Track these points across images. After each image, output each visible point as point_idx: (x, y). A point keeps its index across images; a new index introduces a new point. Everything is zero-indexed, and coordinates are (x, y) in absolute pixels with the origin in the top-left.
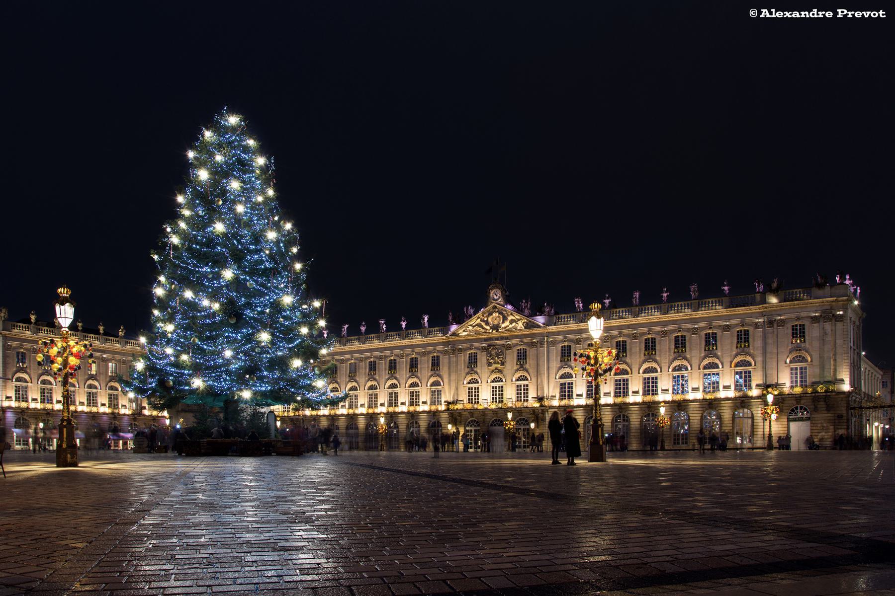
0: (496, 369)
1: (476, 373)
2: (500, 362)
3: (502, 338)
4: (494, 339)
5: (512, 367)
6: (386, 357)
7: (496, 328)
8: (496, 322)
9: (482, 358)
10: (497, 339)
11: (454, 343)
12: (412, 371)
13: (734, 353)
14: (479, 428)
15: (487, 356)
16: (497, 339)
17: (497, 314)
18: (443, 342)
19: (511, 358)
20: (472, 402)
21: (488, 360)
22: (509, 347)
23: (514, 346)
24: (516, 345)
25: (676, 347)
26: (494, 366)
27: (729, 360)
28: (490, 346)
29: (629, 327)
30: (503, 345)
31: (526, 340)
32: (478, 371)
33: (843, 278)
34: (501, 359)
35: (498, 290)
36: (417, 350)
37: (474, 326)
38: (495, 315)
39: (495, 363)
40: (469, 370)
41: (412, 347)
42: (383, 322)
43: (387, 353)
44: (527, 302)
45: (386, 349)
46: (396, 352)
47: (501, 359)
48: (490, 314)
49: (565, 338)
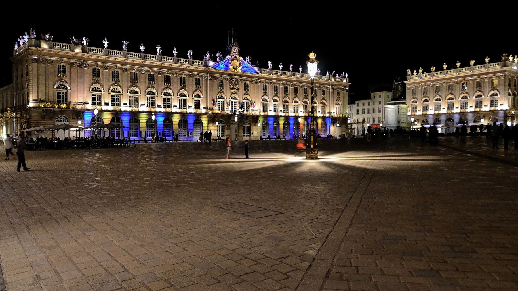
0: (234, 92)
1: (223, 92)
2: (236, 88)
3: (238, 75)
4: (233, 75)
5: (243, 92)
6: (163, 73)
7: (235, 69)
8: (235, 66)
9: (227, 84)
10: (235, 75)
11: (211, 73)
12: (182, 86)
13: (321, 98)
14: (243, 125)
15: (230, 84)
16: (235, 75)
17: (236, 61)
18: (203, 71)
19: (242, 86)
20: (220, 109)
21: (230, 86)
22: (241, 81)
23: (243, 81)
24: (244, 80)
25: (305, 93)
26: (233, 90)
27: (320, 101)
28: (232, 78)
29: (290, 81)
30: (237, 79)
31: (250, 79)
32: (225, 92)
33: (345, 74)
34: (237, 87)
35: (236, 47)
36: (186, 72)
37: (224, 65)
38: (235, 61)
39: (234, 88)
40: (219, 90)
41: (183, 70)
42: (160, 47)
43: (164, 70)
44: (250, 58)
45: (163, 67)
46: (171, 71)
47: (237, 87)
48: (233, 60)
49: (265, 81)
